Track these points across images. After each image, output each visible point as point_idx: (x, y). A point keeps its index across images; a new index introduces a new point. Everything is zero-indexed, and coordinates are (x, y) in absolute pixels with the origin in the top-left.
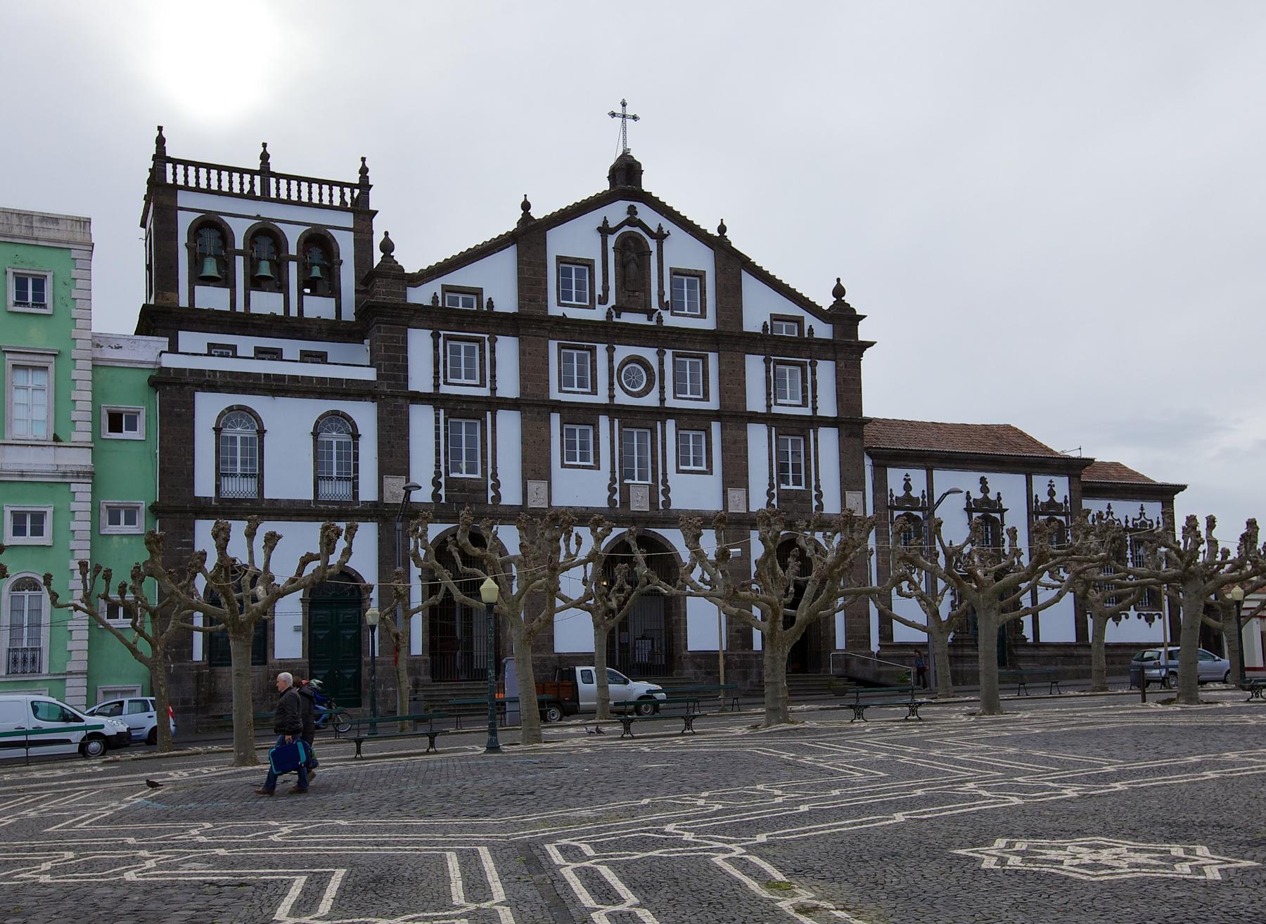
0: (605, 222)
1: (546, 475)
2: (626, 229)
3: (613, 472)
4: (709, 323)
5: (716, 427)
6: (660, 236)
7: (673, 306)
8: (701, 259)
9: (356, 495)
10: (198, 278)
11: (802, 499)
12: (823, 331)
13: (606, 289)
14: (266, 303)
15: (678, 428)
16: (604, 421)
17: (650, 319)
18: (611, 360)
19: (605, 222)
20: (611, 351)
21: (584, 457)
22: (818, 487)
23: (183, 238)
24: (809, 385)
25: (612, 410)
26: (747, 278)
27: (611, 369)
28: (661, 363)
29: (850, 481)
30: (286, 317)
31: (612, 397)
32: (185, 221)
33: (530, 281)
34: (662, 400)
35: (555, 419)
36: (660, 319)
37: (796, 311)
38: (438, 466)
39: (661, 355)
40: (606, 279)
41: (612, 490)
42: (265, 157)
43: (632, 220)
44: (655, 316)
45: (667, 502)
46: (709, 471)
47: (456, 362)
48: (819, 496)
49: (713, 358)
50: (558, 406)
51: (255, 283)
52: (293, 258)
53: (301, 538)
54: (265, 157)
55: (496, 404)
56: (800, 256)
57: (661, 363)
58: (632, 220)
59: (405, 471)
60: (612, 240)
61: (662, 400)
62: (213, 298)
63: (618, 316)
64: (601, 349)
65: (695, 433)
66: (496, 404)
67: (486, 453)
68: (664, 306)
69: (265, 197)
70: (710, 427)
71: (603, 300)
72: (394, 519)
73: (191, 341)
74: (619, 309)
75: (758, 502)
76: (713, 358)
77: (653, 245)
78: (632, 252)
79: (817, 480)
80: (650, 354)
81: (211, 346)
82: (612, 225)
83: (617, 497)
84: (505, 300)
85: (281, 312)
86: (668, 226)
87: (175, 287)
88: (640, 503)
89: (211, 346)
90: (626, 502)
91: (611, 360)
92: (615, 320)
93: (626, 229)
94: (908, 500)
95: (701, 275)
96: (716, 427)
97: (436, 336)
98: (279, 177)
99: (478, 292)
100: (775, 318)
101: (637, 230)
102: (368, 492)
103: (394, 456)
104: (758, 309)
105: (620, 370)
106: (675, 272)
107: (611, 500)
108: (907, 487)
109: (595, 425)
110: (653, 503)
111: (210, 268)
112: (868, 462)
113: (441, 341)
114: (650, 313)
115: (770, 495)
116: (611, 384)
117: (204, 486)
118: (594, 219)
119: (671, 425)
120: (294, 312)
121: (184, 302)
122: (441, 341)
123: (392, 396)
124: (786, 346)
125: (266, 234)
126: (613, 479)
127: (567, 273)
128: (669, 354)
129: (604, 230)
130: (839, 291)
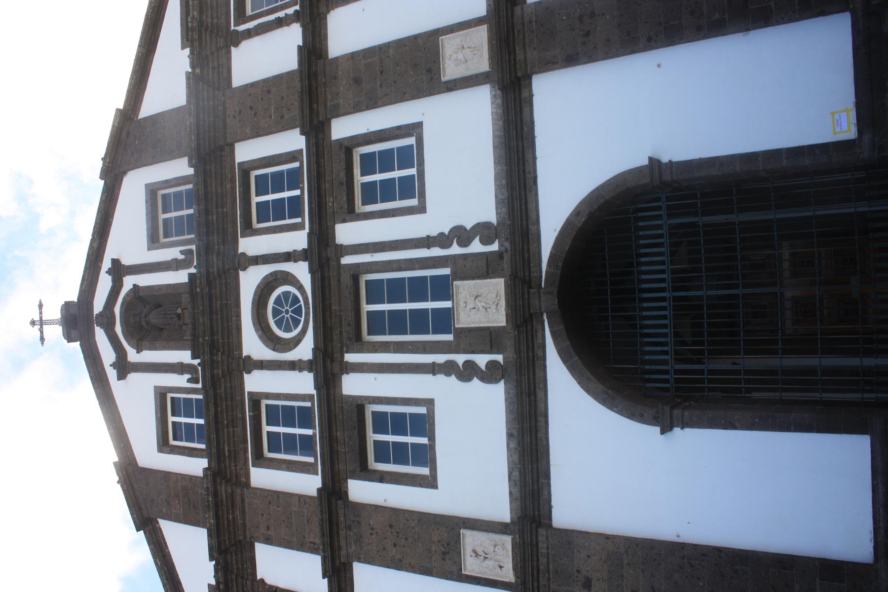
2: (118, 329)
3: (433, 369)
5: (343, 128)
15: (351, 215)
16: (353, 385)
18: (263, 365)
19: (114, 365)
25: (327, 367)
26: (147, 110)
28: (258, 260)
35: (360, 491)
41: (468, 372)
45: (484, 231)
46: (415, 129)
57: (258, 260)
60: (133, 356)
65: (357, 171)
70: (340, 142)
77: (129, 282)
80: (249, 281)
83: (482, 360)
88: (483, 303)
90: (487, 339)
91: (263, 365)
93: (118, 329)
96: (343, 128)
106: (154, 241)
107: (490, 375)
109: (359, 405)
110: (484, 267)
119: (347, 233)
126: (448, 369)
128: (249, 245)
129: (124, 368)
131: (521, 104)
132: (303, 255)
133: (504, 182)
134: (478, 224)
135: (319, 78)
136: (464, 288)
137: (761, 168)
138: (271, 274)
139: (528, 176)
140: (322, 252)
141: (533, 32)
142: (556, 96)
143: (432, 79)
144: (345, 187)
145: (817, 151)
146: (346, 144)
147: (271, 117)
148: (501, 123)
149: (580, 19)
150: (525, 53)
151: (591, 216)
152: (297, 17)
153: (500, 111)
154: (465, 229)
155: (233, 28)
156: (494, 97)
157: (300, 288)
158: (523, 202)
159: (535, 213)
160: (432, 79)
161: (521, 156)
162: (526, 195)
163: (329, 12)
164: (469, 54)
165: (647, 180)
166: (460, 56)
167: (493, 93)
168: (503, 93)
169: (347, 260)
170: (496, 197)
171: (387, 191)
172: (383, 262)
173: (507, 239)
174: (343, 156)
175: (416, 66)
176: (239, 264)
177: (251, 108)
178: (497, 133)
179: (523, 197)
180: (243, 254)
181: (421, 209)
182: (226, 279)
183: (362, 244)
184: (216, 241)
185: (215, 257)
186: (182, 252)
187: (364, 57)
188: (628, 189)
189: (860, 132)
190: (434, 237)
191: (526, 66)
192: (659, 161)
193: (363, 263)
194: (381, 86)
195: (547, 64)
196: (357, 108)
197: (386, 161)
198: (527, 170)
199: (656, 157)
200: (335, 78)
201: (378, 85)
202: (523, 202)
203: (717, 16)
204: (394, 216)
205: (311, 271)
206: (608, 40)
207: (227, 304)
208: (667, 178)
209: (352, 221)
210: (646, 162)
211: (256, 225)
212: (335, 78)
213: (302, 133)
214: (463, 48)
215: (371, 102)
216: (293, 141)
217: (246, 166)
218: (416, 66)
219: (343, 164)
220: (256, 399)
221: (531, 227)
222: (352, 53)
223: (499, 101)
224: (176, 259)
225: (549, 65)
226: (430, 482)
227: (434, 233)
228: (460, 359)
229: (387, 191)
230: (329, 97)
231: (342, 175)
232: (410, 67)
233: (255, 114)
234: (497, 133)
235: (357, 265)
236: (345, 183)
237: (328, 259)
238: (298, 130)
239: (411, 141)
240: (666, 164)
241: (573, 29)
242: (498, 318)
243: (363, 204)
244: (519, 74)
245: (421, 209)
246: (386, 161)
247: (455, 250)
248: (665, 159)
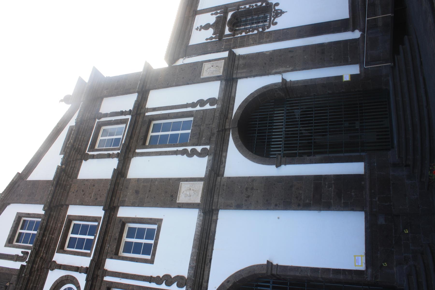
15: (116, 255)
22: (193, 105)
24: (113, 118)
46: (158, 222)
48: (202, 103)
65: (125, 234)
70: (121, 218)
75: (197, 167)
80: (53, 276)
94: (218, 26)
96: (124, 212)
108: (207, 27)
115: (193, 153)
119: (111, 264)
131: (211, 222)
132: (85, 270)
133: (195, 258)
134: (178, 276)
135: (120, 186)
137: (320, 276)
138: (66, 276)
139: (207, 257)
140: (95, 272)
141: (224, 190)
142: (229, 222)
143: (172, 200)
144: (116, 241)
145: (347, 273)
146: (123, 220)
147: (91, 197)
148: (200, 229)
149: (247, 189)
150: (218, 199)
151: (234, 284)
152: (118, 156)
153: (201, 223)
154: (171, 277)
155: (87, 152)
156: (199, 216)
157: (78, 287)
158: (202, 270)
159: (207, 277)
160: (172, 200)
161: (206, 247)
162: (204, 266)
163: (133, 157)
164: (192, 193)
165: (264, 272)
166: (188, 193)
167: (199, 214)
168: (204, 215)
169: (107, 279)
170: (190, 264)
171: (137, 248)
172: (125, 284)
173: (190, 287)
174: (120, 226)
175: (166, 192)
176: (50, 266)
177: (83, 191)
178: (197, 233)
179: (203, 268)
180: (55, 262)
181: (151, 262)
182: (40, 273)
183: (117, 272)
184: (43, 251)
185: (39, 259)
186: (22, 252)
187: (143, 182)
188: (255, 274)
189: (367, 267)
190: (154, 278)
191: (217, 205)
192: (272, 263)
193: (115, 282)
194: (147, 197)
195: (227, 206)
196: (133, 205)
197: (140, 234)
198: (208, 254)
199: (271, 261)
200: (127, 188)
201: (147, 196)
202: (202, 270)
203: (308, 201)
204: (137, 262)
205: (87, 280)
206: (257, 202)
207: (36, 287)
208: (274, 272)
209: (115, 259)
210: (265, 263)
211: (66, 248)
212: (127, 188)
213: (104, 209)
214: (190, 189)
215: (141, 204)
216: (98, 212)
217: (71, 218)
218: (166, 192)
219: (119, 230)
221: (203, 283)
222: (138, 179)
223: (201, 218)
224: (18, 255)
225: (228, 207)
227: (155, 275)
229: (137, 248)
230: (122, 196)
231: (117, 235)
232: (164, 192)
233: (84, 194)
234: (197, 233)
235: (112, 283)
236: (117, 240)
237: (97, 276)
238: (102, 207)
239: (155, 227)
240: (275, 265)
241: (242, 193)
243: (124, 252)
244: (213, 208)
245: (151, 262)
246: (140, 234)
248: (275, 263)
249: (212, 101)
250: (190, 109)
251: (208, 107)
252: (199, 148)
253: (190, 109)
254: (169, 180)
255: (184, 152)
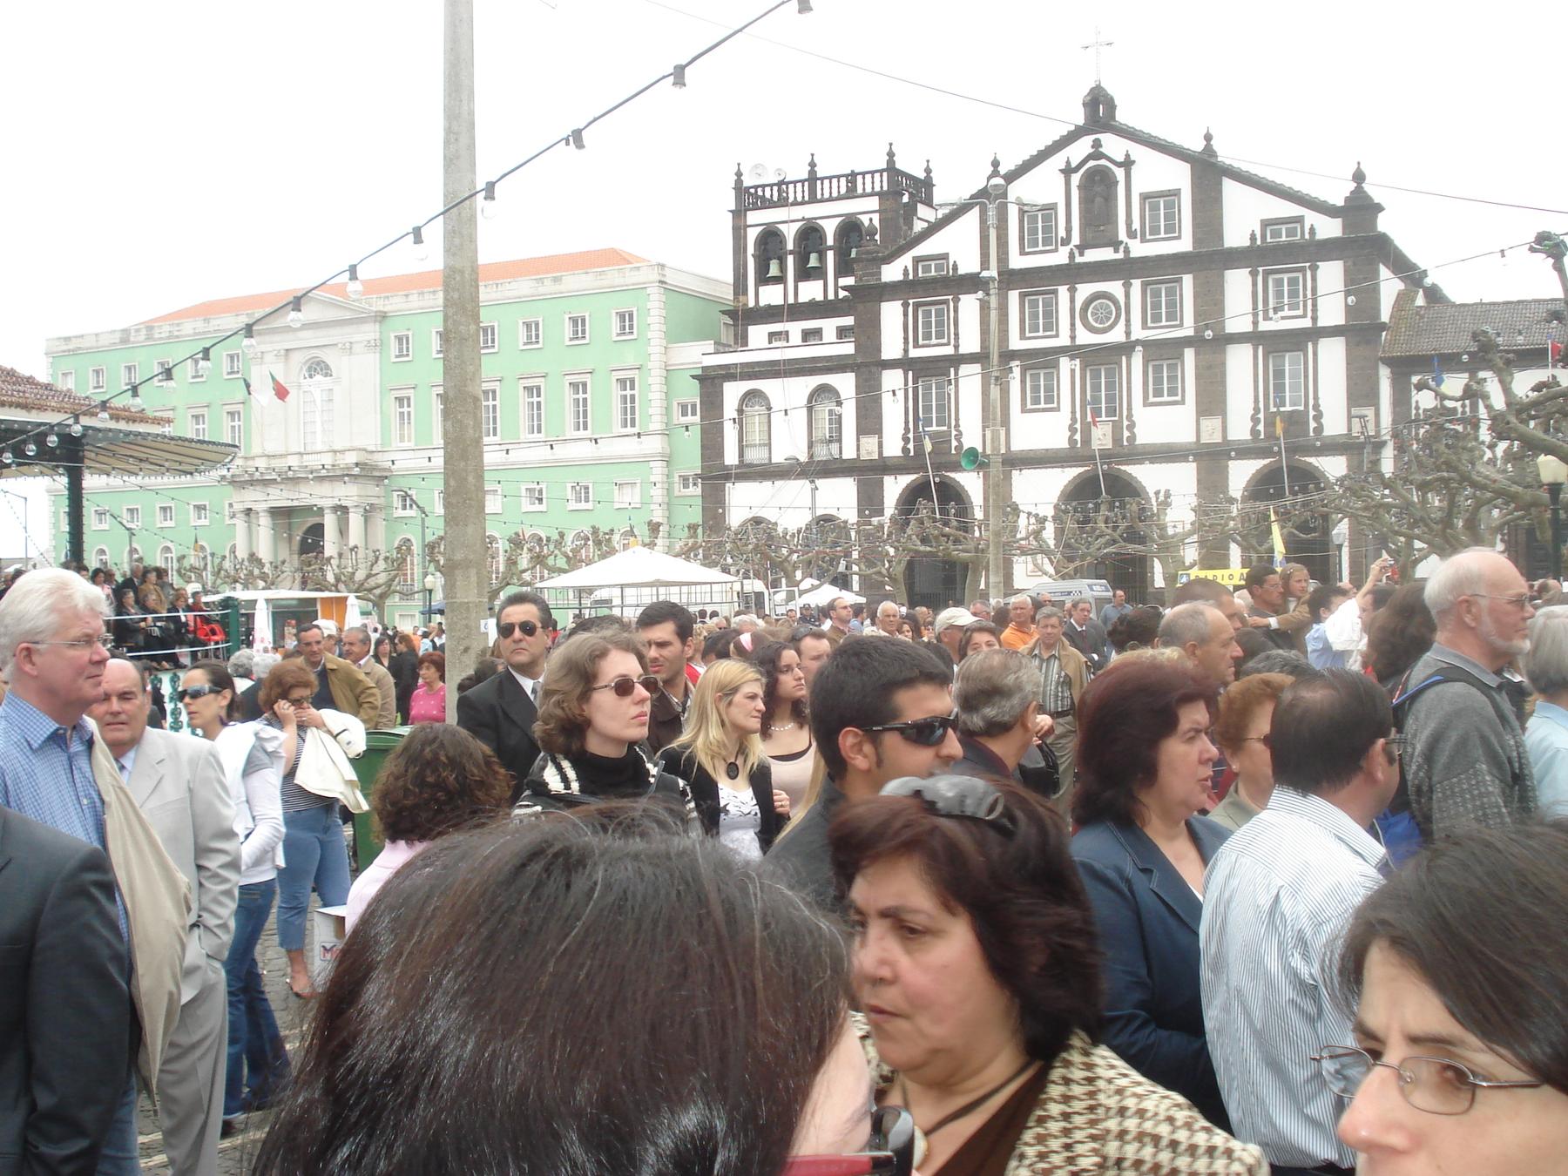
0: (1068, 162)
1: (1006, 422)
2: (1091, 163)
3: (1073, 412)
4: (1185, 244)
5: (1189, 354)
6: (1127, 164)
7: (1149, 232)
8: (1177, 176)
9: (881, 453)
10: (763, 279)
11: (1295, 421)
12: (1329, 228)
13: (1069, 230)
14: (811, 291)
17: (1116, 251)
18: (1072, 300)
19: (1068, 162)
20: (1072, 291)
21: (1049, 399)
22: (1316, 406)
23: (751, 249)
25: (1073, 351)
26: (1229, 186)
27: (1072, 310)
28: (1127, 295)
29: (1361, 393)
30: (826, 302)
31: (1073, 338)
32: (752, 235)
33: (992, 238)
34: (1128, 334)
36: (1127, 251)
37: (1289, 209)
38: (907, 422)
39: (1127, 286)
40: (1071, 222)
41: (1072, 430)
42: (812, 165)
43: (1097, 154)
44: (1122, 249)
45: (1132, 438)
47: (927, 324)
49: (1188, 280)
50: (1014, 355)
51: (804, 274)
52: (830, 248)
53: (797, 489)
54: (812, 165)
55: (958, 360)
56: (1297, 151)
57: (1127, 295)
58: (1097, 154)
59: (878, 431)
60: (1076, 179)
61: (1128, 334)
62: (772, 295)
63: (1081, 254)
64: (1063, 291)
66: (958, 360)
67: (946, 410)
68: (1131, 234)
69: (813, 199)
71: (1066, 242)
72: (869, 473)
73: (758, 334)
74: (1082, 248)
75: (1240, 431)
76: (1188, 280)
77: (1120, 173)
78: (1098, 187)
79: (1316, 398)
80: (1115, 288)
81: (772, 335)
82: (1073, 165)
83: (1078, 437)
84: (968, 264)
85: (820, 297)
86: (1138, 152)
87: (745, 292)
88: (1101, 438)
89: (772, 335)
90: (1087, 440)
91: (1072, 300)
92: (1078, 259)
93: (1091, 163)
95: (1176, 193)
97: (905, 305)
98: (822, 179)
99: (945, 257)
100: (1265, 224)
101: (1103, 162)
102: (849, 453)
103: (870, 421)
104: (1243, 217)
105: (1085, 309)
106: (1145, 197)
107: (1072, 441)
110: (1117, 439)
111: (774, 270)
112: (1384, 374)
113: (910, 309)
114: (1116, 244)
115: (1255, 421)
116: (1073, 325)
117: (731, 457)
118: (1058, 161)
119: (1137, 359)
120: (831, 296)
121: (751, 304)
122: (910, 309)
123: (867, 366)
124: (1280, 254)
125: (810, 234)
126: (1074, 420)
127: (1034, 220)
130: (1359, 177)
136: (1108, 429)
220: (1055, 292)
226: (1024, 410)
228: (1078, 426)
232: (1212, 401)
242: (1096, 445)
247: (1126, 423)
249: (1319, 429)
250: (1311, 402)
251: (1313, 424)
252: (1261, 427)
253: (1311, 402)
254: (1224, 402)
255: (1257, 410)
